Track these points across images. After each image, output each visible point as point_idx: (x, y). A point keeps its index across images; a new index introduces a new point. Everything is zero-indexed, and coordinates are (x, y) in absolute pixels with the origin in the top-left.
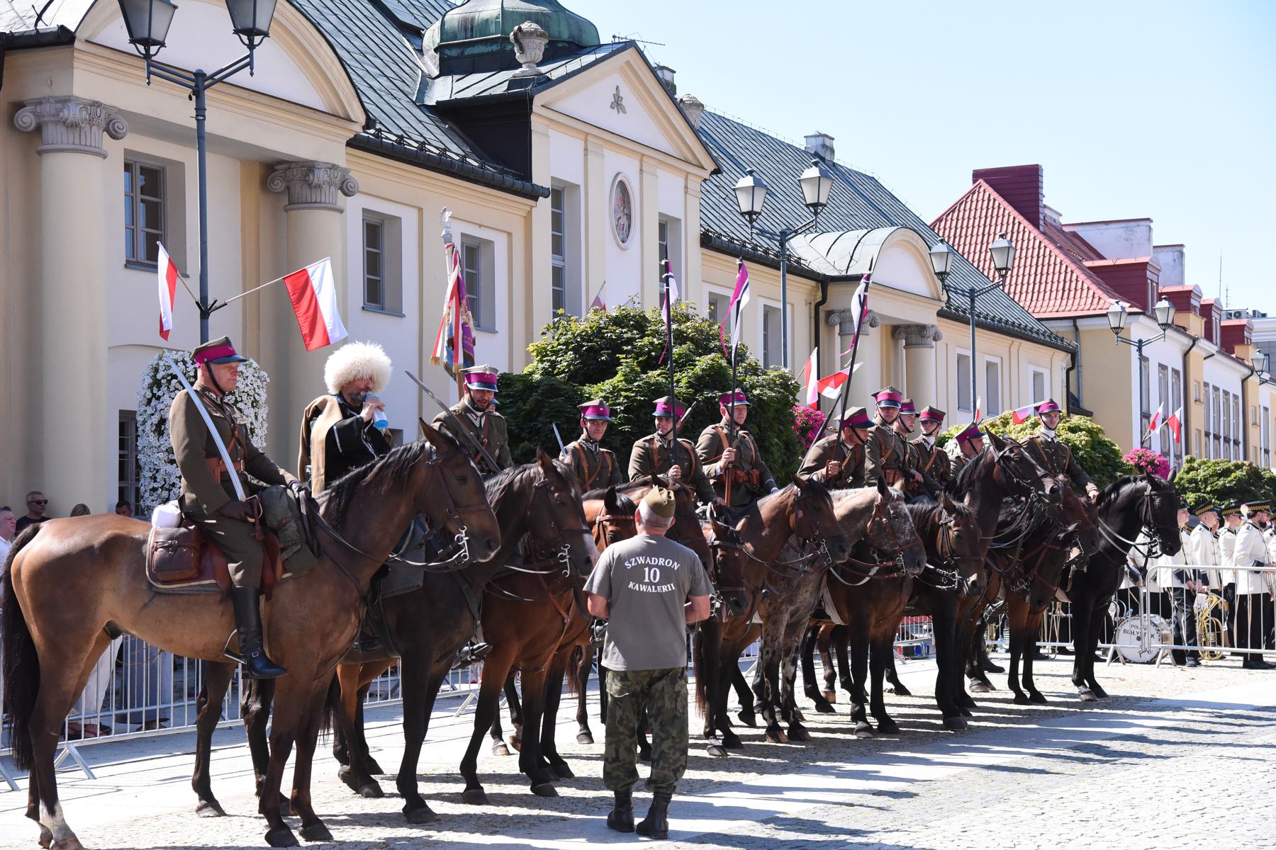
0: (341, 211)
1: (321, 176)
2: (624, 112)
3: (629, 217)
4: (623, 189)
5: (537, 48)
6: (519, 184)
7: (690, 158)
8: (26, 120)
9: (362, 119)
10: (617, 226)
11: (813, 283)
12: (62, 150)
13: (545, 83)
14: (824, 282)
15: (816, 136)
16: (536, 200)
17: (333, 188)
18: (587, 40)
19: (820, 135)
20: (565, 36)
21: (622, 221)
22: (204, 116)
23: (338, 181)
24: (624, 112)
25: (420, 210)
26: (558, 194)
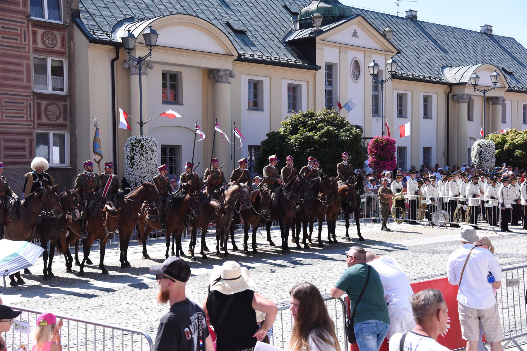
0: (230, 83)
1: (222, 73)
2: (358, 37)
3: (359, 72)
4: (357, 64)
5: (319, 21)
6: (312, 67)
7: (387, 49)
8: (126, 66)
9: (237, 55)
10: (353, 75)
11: (447, 86)
12: (134, 74)
13: (321, 32)
14: (451, 85)
15: (484, 26)
16: (317, 70)
17: (227, 76)
18: (347, 14)
19: (488, 26)
20: (338, 14)
21: (356, 73)
22: (141, 70)
23: (228, 74)
24: (358, 37)
25: (271, 78)
26: (330, 67)
